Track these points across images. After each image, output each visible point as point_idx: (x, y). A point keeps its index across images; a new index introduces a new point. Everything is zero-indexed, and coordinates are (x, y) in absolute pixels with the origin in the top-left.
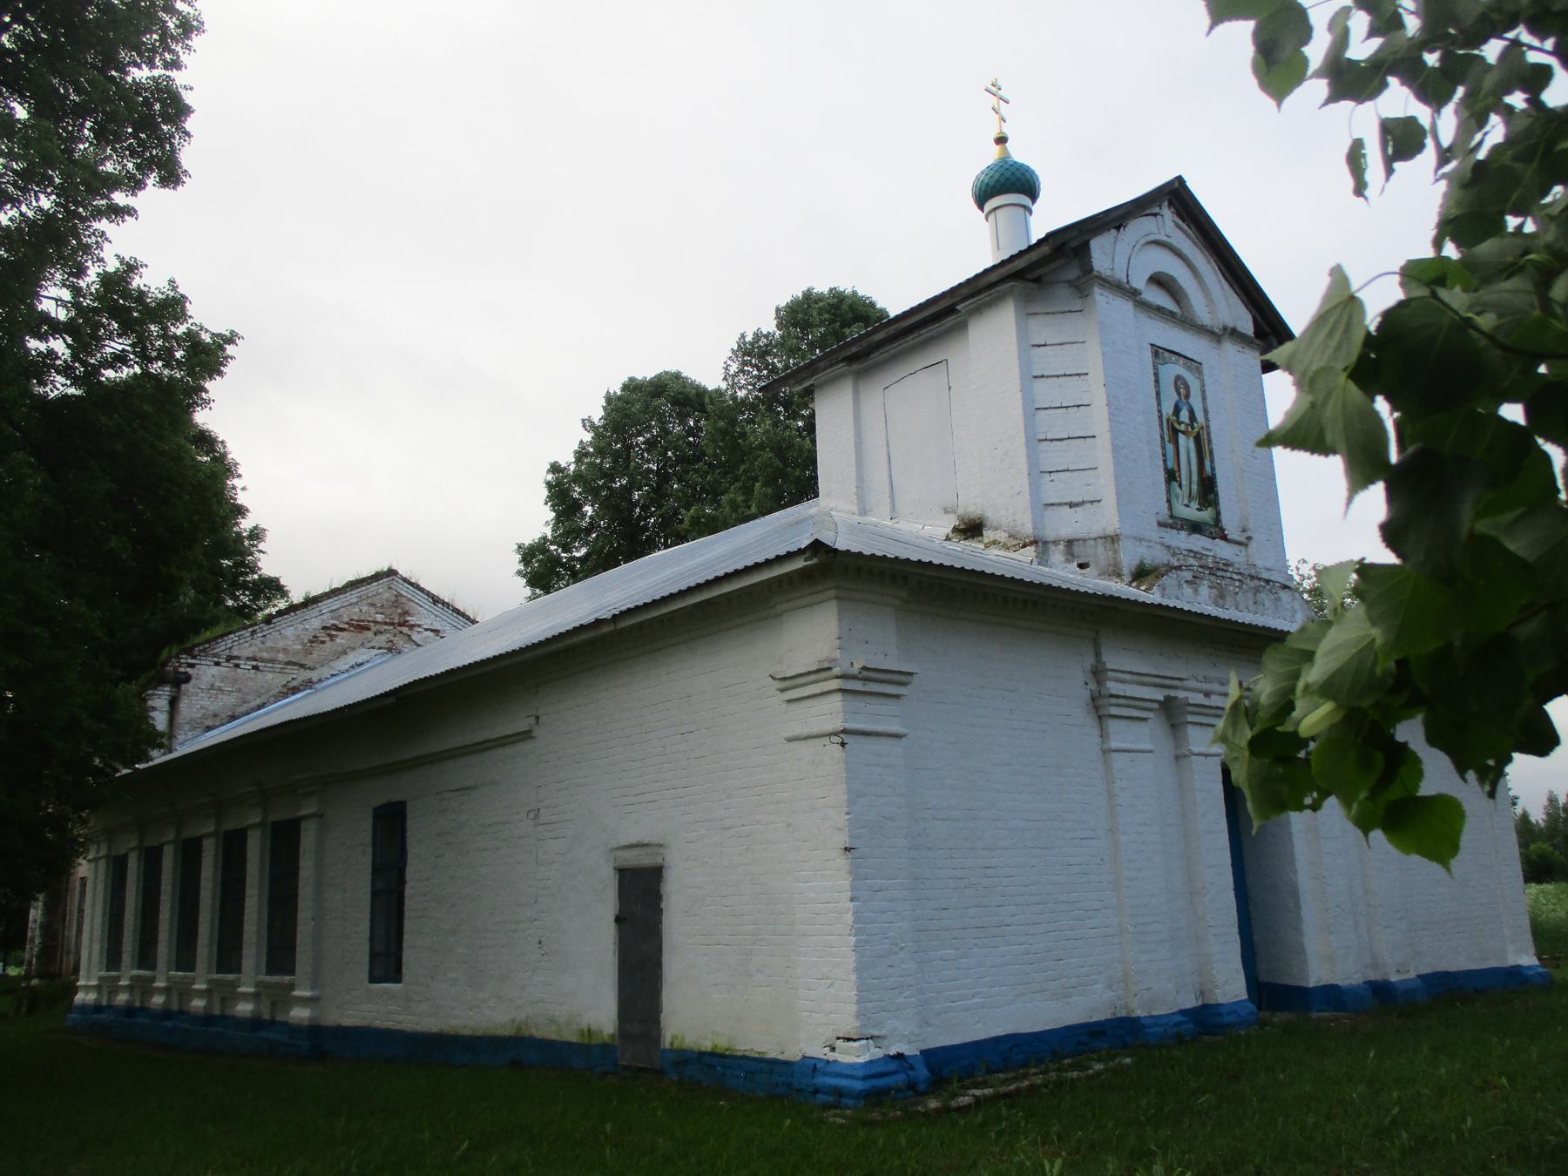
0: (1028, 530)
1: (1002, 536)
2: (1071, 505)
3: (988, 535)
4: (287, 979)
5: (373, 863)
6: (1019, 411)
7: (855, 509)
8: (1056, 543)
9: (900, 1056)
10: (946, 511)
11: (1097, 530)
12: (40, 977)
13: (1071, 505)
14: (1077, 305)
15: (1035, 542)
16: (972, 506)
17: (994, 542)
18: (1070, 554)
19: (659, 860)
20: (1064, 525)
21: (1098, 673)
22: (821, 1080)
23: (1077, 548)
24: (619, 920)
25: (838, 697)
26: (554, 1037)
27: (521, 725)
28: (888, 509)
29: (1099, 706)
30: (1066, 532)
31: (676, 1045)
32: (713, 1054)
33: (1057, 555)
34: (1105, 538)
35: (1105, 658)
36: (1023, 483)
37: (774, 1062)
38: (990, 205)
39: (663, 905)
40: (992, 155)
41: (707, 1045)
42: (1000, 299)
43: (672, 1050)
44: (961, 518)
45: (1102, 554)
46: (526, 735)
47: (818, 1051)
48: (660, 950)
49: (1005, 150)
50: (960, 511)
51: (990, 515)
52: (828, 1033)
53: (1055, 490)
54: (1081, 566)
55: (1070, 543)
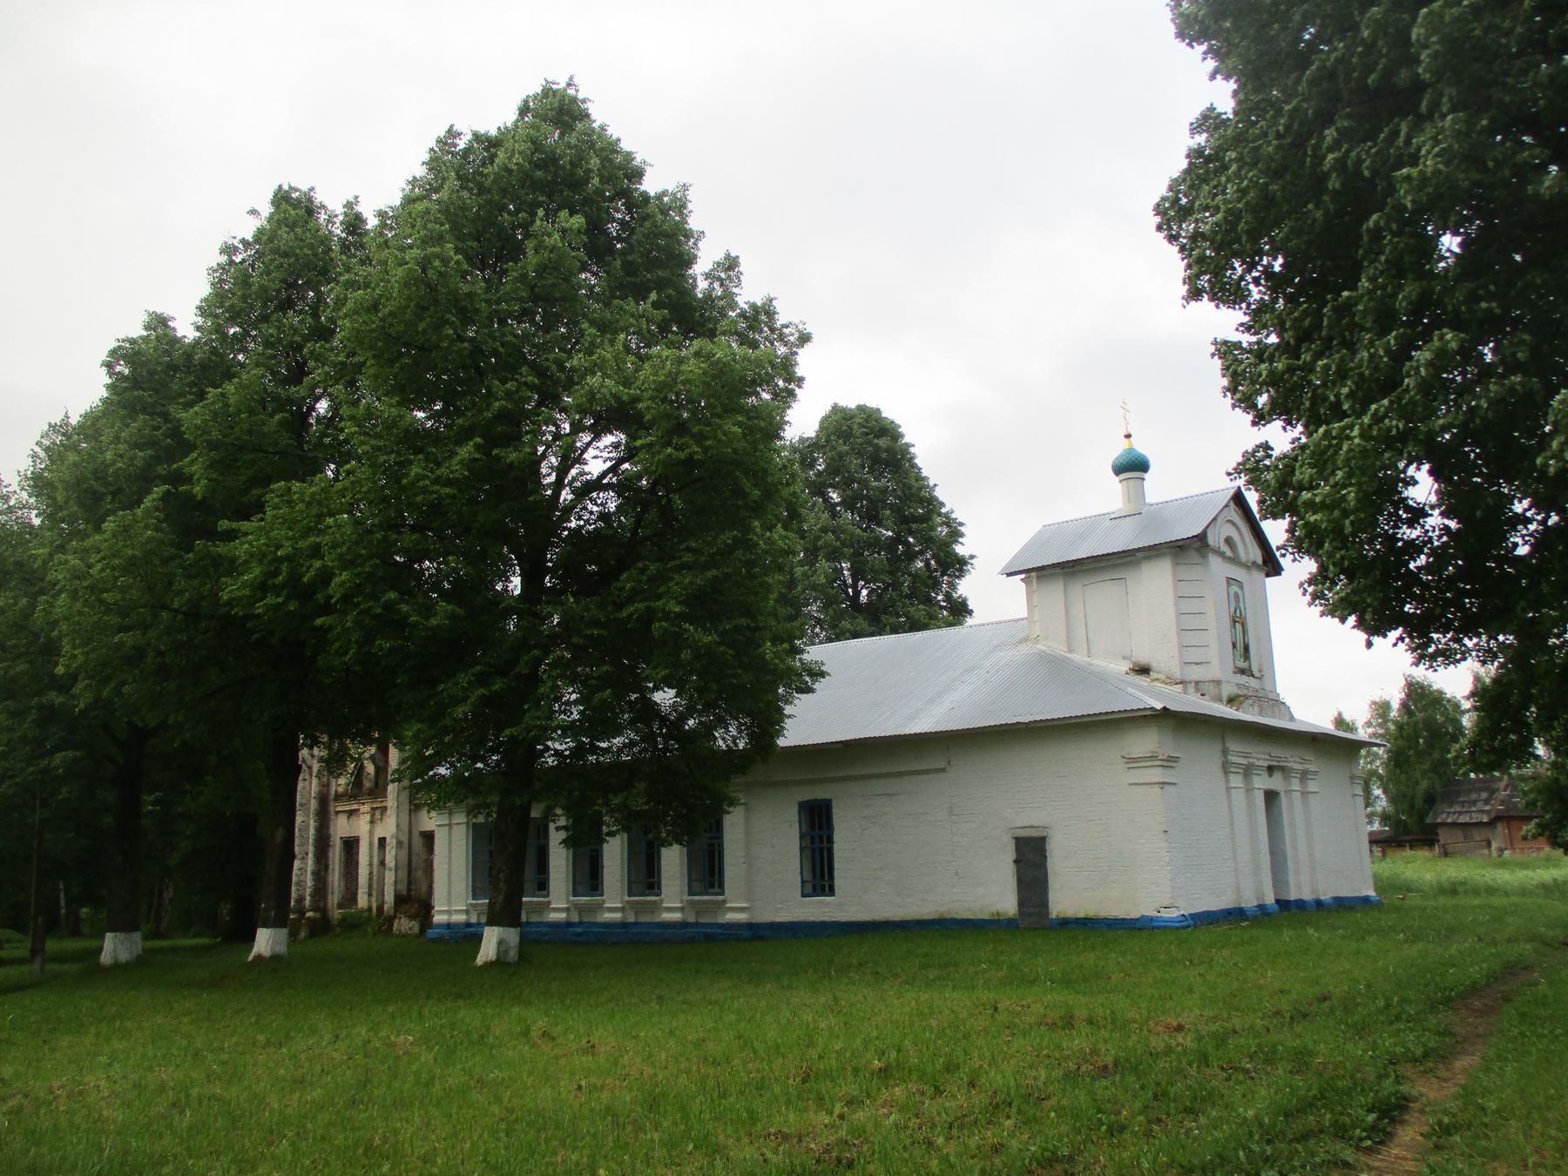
0: (1178, 675)
1: (1162, 677)
2: (1197, 664)
3: (1153, 675)
4: (721, 898)
5: (800, 832)
6: (1173, 615)
7: (1066, 650)
8: (1190, 682)
9: (1183, 915)
10: (1124, 658)
11: (1209, 677)
12: (314, 910)
13: (1197, 664)
14: (1199, 561)
15: (1181, 683)
16: (1143, 658)
17: (1157, 679)
18: (1197, 690)
19: (1045, 834)
20: (1195, 673)
21: (1225, 752)
22: (1155, 924)
23: (1200, 686)
24: (1016, 862)
25: (1160, 768)
26: (971, 917)
27: (942, 764)
28: (1086, 652)
29: (1226, 768)
30: (1194, 677)
31: (1061, 916)
32: (1085, 919)
33: (1191, 689)
34: (1213, 681)
35: (1228, 745)
36: (1175, 652)
37: (1123, 919)
38: (1123, 476)
39: (1047, 854)
40: (1124, 445)
41: (1082, 915)
42: (1164, 555)
43: (1058, 918)
44: (1135, 664)
45: (1211, 689)
46: (943, 770)
47: (1154, 914)
48: (1047, 874)
49: (1130, 443)
50: (1133, 659)
51: (1154, 664)
52: (1157, 905)
53: (1193, 655)
54: (1202, 695)
55: (1197, 683)
